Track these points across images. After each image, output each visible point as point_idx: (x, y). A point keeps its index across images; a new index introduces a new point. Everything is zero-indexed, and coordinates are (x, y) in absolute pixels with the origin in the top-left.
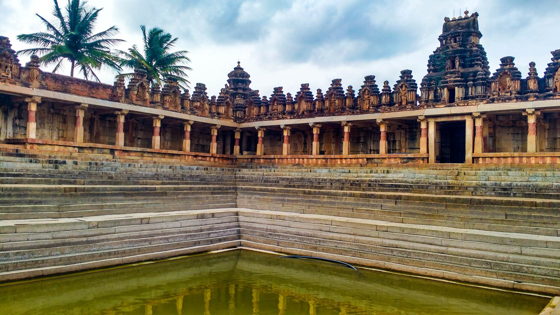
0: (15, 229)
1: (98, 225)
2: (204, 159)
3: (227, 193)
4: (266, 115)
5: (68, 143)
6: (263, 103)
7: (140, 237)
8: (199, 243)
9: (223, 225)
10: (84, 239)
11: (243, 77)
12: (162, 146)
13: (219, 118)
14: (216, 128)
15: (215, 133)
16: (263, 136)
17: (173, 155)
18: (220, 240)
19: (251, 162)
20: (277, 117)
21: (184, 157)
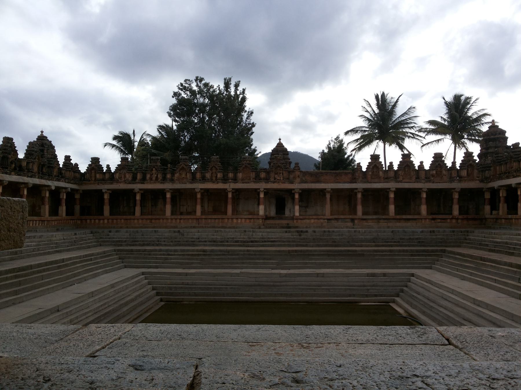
0: (237, 275)
1: (286, 275)
2: (443, 221)
3: (429, 255)
4: (505, 173)
5: (320, 217)
6: (503, 161)
7: (309, 286)
8: (354, 295)
9: (388, 284)
10: (272, 284)
11: (495, 135)
12: (397, 212)
13: (460, 181)
14: (456, 192)
15: (456, 196)
16: (505, 195)
17: (409, 220)
18: (376, 296)
19: (496, 222)
20: (513, 175)
21: (420, 220)
